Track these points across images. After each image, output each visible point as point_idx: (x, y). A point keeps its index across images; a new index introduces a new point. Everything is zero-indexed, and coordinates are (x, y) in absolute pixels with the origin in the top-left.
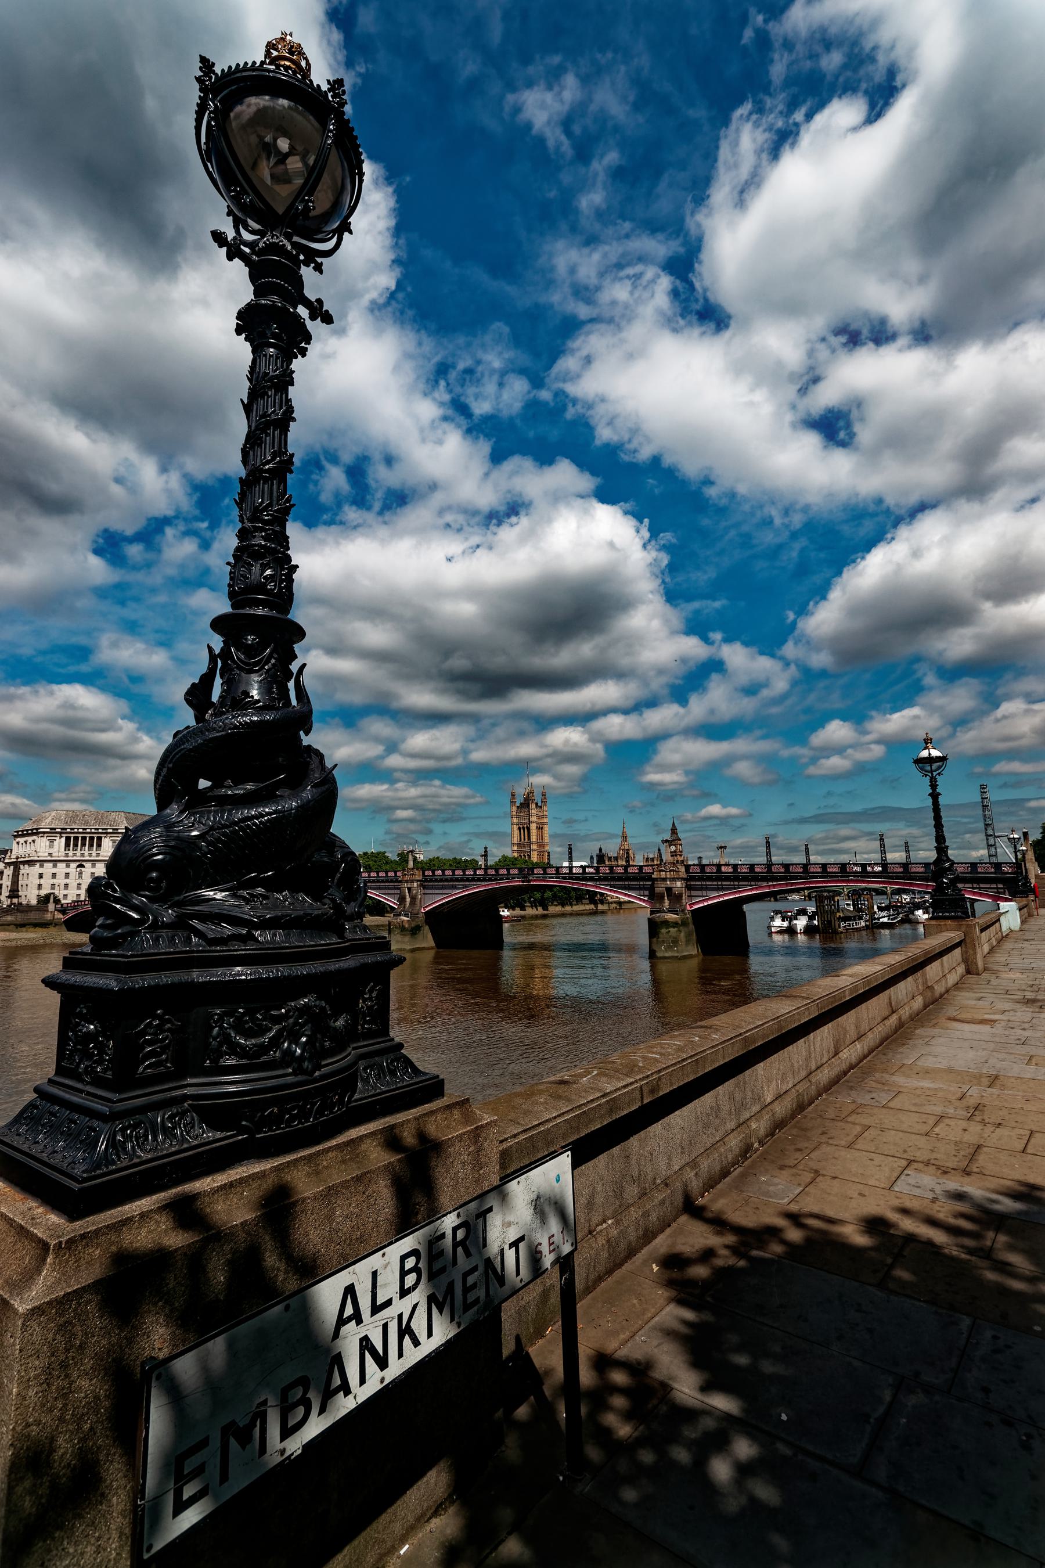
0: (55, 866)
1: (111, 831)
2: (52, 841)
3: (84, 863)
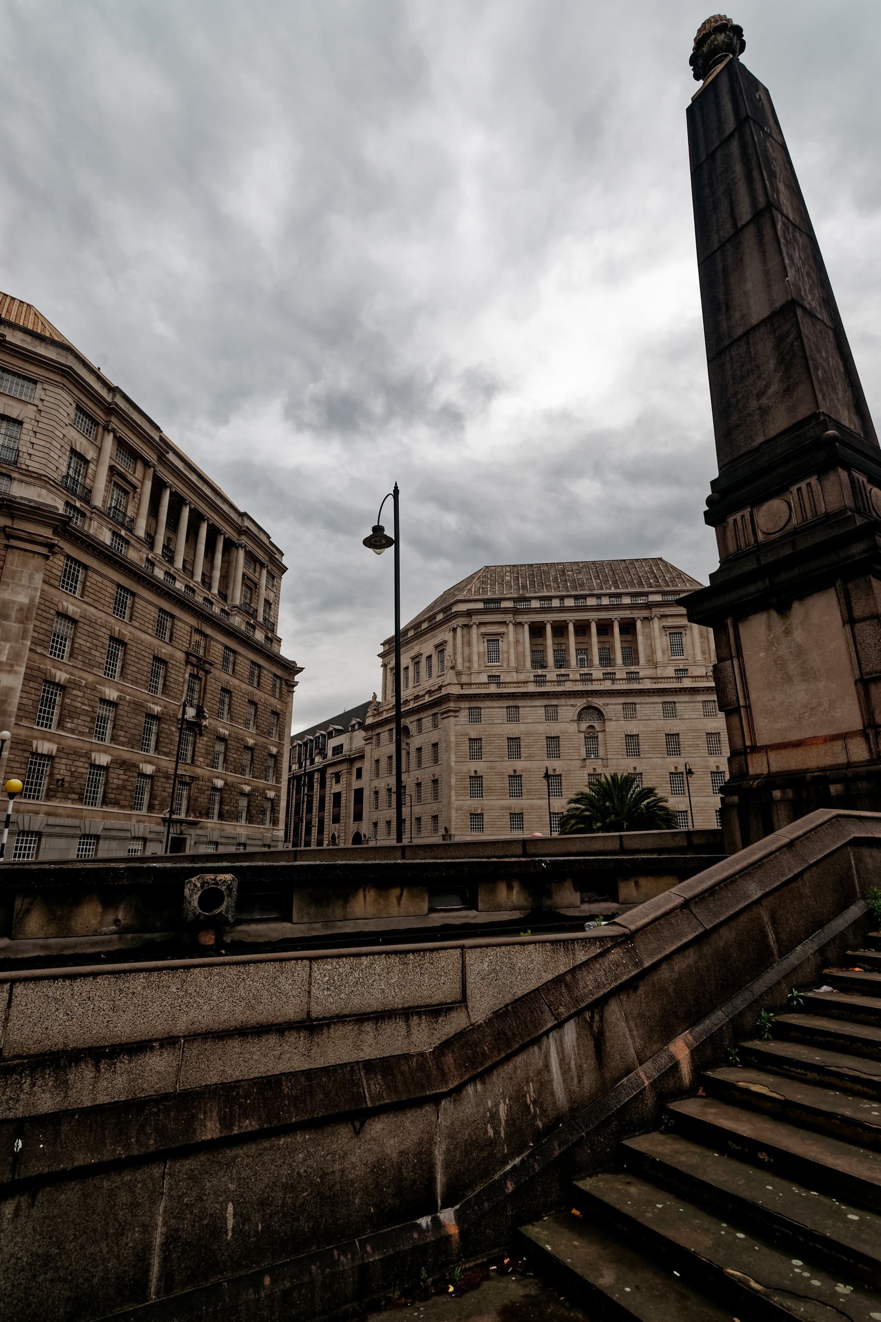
0: (513, 716)
1: (658, 598)
2: (493, 639)
3: (598, 702)
